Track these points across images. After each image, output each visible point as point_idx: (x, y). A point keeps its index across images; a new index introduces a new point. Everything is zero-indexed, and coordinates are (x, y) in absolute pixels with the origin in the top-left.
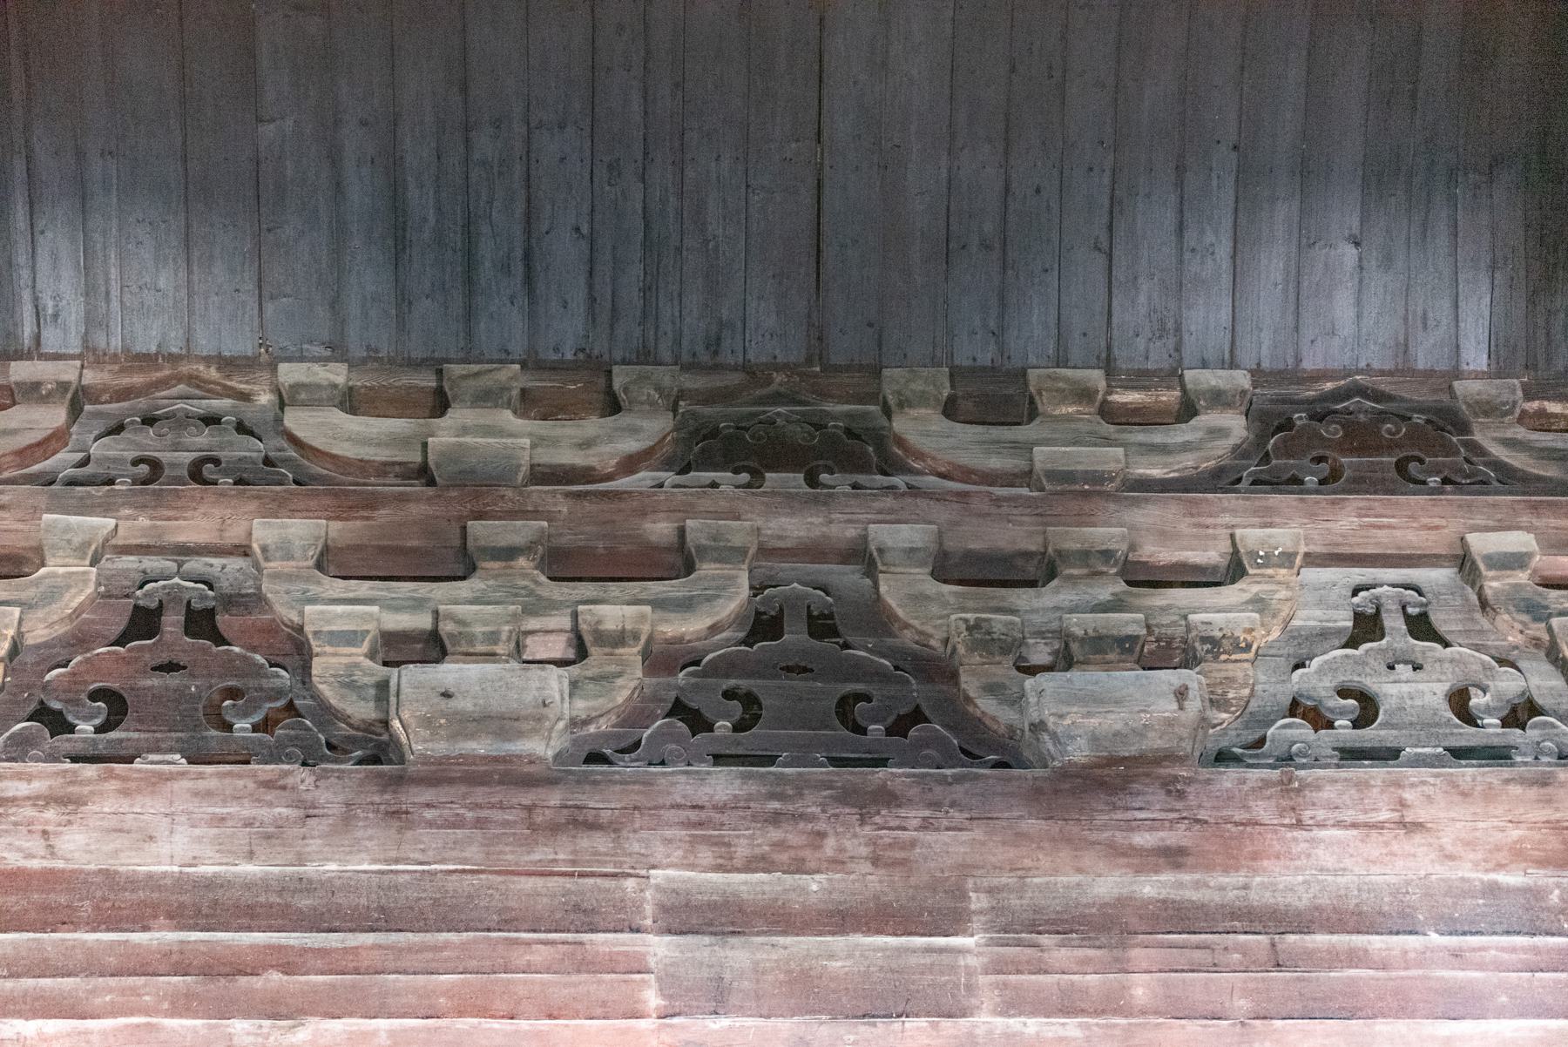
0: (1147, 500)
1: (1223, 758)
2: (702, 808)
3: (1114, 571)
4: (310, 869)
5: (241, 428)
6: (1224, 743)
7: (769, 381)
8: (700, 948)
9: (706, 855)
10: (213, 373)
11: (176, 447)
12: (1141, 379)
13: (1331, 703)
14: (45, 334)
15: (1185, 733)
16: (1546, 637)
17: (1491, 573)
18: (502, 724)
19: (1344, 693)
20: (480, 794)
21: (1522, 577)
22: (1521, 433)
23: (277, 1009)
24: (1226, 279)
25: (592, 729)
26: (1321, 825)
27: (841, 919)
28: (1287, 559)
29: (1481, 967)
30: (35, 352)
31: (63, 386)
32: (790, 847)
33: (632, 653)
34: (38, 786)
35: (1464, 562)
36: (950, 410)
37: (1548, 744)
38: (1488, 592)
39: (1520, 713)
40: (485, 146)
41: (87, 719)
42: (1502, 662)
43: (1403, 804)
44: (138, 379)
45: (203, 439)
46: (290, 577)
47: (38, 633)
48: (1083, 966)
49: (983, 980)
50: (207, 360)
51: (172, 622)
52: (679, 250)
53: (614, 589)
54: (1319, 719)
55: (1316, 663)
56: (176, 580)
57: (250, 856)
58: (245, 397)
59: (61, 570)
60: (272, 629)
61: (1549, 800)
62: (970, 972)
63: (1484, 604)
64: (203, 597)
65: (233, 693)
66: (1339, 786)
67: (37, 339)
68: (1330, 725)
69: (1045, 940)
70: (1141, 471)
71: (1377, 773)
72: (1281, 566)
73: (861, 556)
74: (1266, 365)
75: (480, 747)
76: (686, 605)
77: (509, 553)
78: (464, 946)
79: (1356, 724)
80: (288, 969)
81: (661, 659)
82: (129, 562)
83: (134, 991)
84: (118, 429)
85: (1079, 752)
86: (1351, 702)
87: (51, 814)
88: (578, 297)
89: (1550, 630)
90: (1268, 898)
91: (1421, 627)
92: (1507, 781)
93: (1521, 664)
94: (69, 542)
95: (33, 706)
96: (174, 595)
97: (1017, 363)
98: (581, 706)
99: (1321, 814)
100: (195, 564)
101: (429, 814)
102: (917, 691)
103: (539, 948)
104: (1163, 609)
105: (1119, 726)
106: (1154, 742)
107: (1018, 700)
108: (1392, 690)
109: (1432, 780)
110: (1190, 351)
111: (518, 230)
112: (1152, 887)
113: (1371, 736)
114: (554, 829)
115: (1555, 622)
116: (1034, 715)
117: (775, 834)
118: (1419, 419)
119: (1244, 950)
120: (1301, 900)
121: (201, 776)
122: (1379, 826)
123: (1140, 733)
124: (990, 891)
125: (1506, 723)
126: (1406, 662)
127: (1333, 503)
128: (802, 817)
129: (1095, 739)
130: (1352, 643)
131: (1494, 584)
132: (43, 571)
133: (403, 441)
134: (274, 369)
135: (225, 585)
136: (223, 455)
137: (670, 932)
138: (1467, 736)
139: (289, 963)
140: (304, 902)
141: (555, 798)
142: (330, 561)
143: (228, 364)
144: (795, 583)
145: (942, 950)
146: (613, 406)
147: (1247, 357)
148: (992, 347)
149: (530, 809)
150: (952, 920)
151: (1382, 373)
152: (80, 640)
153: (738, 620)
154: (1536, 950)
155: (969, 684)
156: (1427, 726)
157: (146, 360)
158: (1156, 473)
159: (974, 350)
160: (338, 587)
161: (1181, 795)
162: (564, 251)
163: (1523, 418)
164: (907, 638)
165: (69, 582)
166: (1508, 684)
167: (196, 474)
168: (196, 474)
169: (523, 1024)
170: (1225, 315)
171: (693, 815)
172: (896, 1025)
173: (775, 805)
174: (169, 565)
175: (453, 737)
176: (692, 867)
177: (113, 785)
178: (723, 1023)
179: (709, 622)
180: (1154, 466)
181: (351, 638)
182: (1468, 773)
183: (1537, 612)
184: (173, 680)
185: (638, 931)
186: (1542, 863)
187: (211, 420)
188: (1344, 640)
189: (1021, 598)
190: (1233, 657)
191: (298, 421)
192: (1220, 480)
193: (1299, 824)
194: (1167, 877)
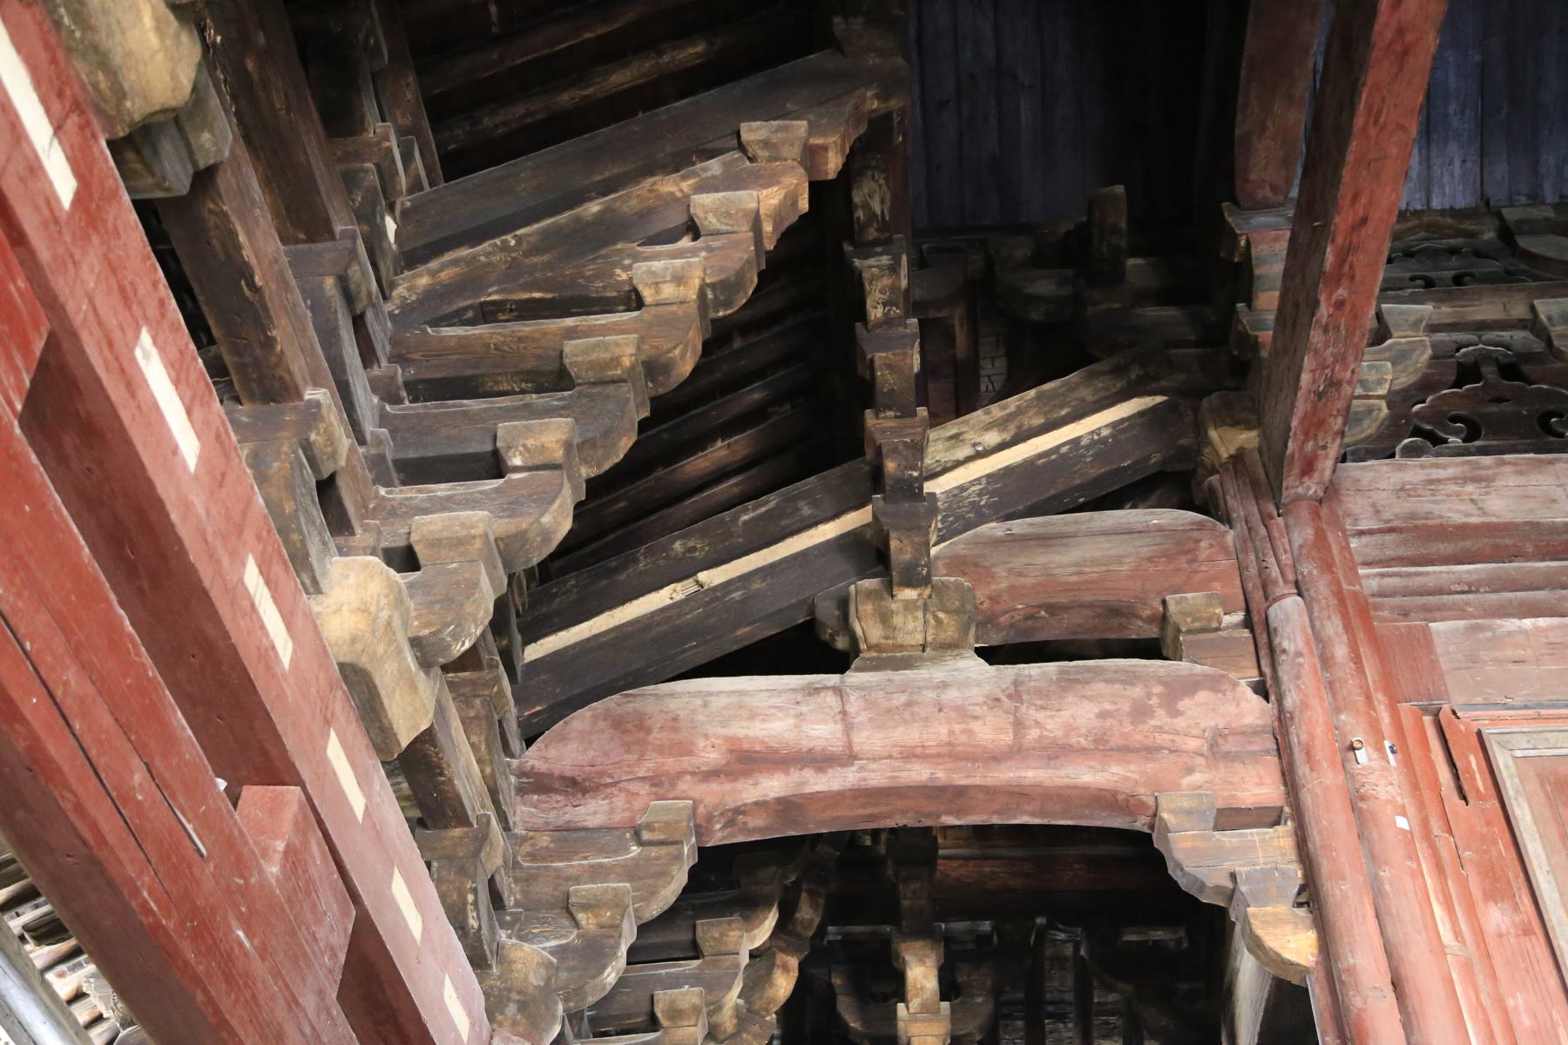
34: (1450, 472)
50: (1442, 212)
51: (1489, 372)
56: (1481, 346)
58: (1470, 235)
59: (1404, 340)
64: (1506, 356)
87: (1470, 488)
94: (1407, 321)
96: (1486, 357)
132: (1389, 342)
136: (1474, 270)
165: (1413, 347)
168: (1458, 280)
174: (1471, 337)
177: (1508, 469)
187: (1454, 251)
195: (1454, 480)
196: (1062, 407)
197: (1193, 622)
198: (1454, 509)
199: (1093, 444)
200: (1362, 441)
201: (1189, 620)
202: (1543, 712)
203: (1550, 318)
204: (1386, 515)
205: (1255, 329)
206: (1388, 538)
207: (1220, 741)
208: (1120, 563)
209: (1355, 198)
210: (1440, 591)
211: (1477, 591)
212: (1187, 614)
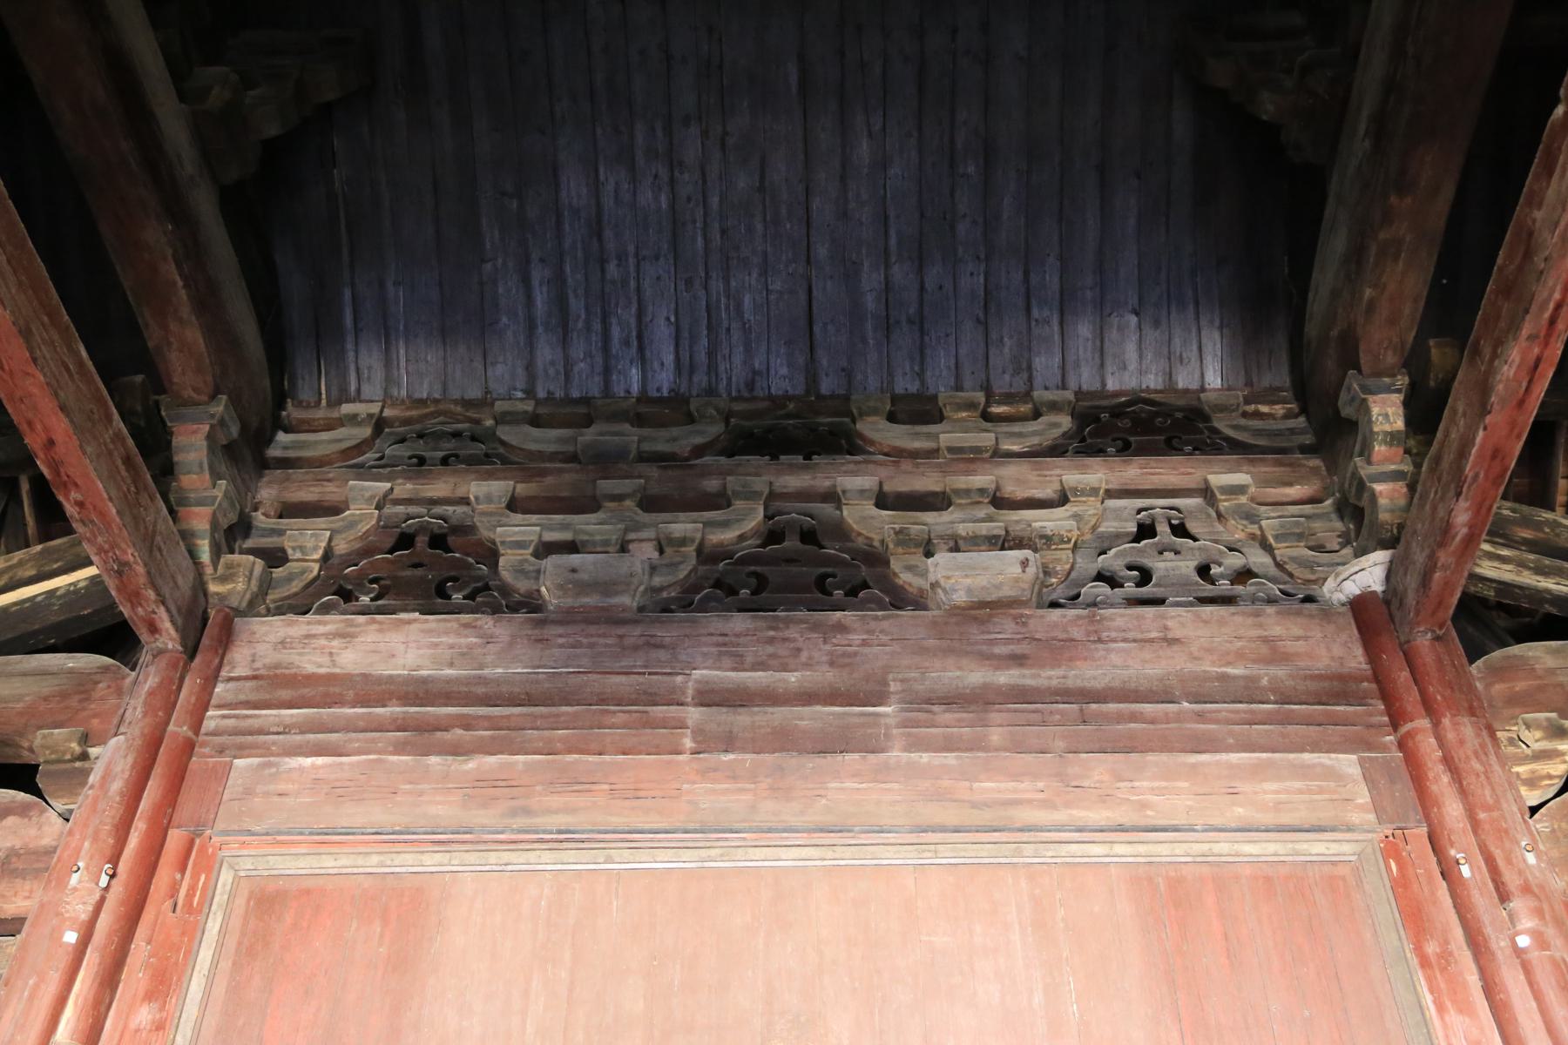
0: (1009, 463)
1: (1054, 605)
2: (726, 635)
3: (986, 501)
4: (486, 672)
5: (474, 439)
6: (1054, 597)
7: (785, 406)
8: (722, 715)
9: (727, 662)
10: (459, 409)
11: (435, 449)
12: (1008, 398)
13: (1122, 574)
14: (363, 388)
15: (1026, 586)
16: (1259, 533)
17: (1223, 497)
18: (606, 587)
19: (1130, 568)
20: (592, 629)
21: (1243, 499)
22: (1243, 422)
23: (456, 750)
24: (1057, 337)
25: (665, 595)
26: (1114, 641)
27: (808, 697)
28: (1094, 491)
29: (1217, 722)
30: (358, 398)
31: (370, 416)
32: (780, 657)
33: (690, 550)
35: (1206, 492)
36: (892, 418)
37: (1261, 594)
38: (1221, 508)
39: (1244, 575)
40: (612, 269)
41: (366, 594)
42: (1231, 550)
43: (1166, 628)
44: (414, 413)
45: (449, 446)
46: (491, 514)
47: (341, 547)
48: (959, 724)
49: (895, 731)
50: (456, 402)
51: (422, 541)
52: (728, 330)
53: (682, 515)
54: (1112, 581)
55: (1113, 551)
56: (426, 518)
57: (451, 665)
58: (477, 422)
59: (358, 512)
60: (480, 543)
61: (1261, 626)
62: (887, 727)
63: (1220, 516)
64: (441, 527)
65: (454, 579)
66: (1126, 619)
67: (359, 391)
68: (1122, 586)
69: (936, 708)
70: (1006, 447)
71: (1149, 611)
72: (1090, 496)
73: (833, 497)
74: (1085, 387)
75: (590, 600)
76: (725, 524)
77: (619, 498)
78: (575, 714)
79: (1139, 585)
80: (467, 727)
81: (708, 556)
82: (400, 509)
83: (373, 741)
84: (402, 441)
85: (960, 598)
86: (1136, 573)
87: (335, 643)
88: (669, 359)
89: (1261, 528)
90: (1079, 683)
91: (1180, 530)
92: (1234, 614)
93: (1243, 550)
94: (363, 496)
95: (334, 588)
96: (423, 528)
97: (932, 391)
98: (657, 581)
99: (1113, 634)
100: (438, 510)
101: (561, 641)
102: (864, 572)
103: (619, 715)
104: (1017, 522)
105: (984, 583)
106: (1007, 592)
107: (924, 574)
108: (1161, 566)
109: (1185, 614)
110: (1038, 381)
111: (633, 321)
112: (1006, 677)
113: (1146, 591)
114: (636, 648)
115: (1264, 523)
116: (932, 578)
117: (770, 649)
118: (1179, 415)
119: (1062, 713)
120: (1098, 684)
121: (427, 621)
122: (1152, 641)
123: (998, 587)
124: (902, 681)
126: (1171, 550)
127: (1125, 461)
128: (785, 640)
129: (969, 591)
130: (1137, 538)
131: (1224, 505)
132: (348, 513)
133: (560, 440)
134: (492, 404)
135: (454, 521)
136: (462, 453)
137: (702, 705)
138: (1208, 590)
139: (467, 724)
140: (481, 690)
141: (637, 631)
142: (514, 505)
143: (468, 404)
144: (794, 514)
145: (870, 714)
146: (690, 419)
147: (1072, 383)
148: (917, 383)
149: (621, 637)
150: (880, 698)
151: (1156, 391)
152: (367, 552)
153: (755, 533)
154: (1252, 712)
155: (895, 565)
156: (1184, 584)
157: (422, 402)
158: (1015, 448)
159: (905, 384)
160: (519, 517)
161: (1024, 624)
162: (662, 332)
163: (1245, 415)
164: (860, 542)
165: (362, 518)
166: (1235, 561)
167: (445, 461)
169: (607, 758)
170: (1057, 360)
171: (721, 639)
172: (839, 757)
173: (772, 633)
174: (422, 510)
175: (578, 595)
176: (719, 669)
177: (375, 626)
178: (731, 756)
179: (738, 533)
180: (1014, 444)
181: (520, 545)
182: (1208, 610)
183: (1252, 518)
184: (419, 572)
185: (682, 704)
186: (1255, 661)
187: (457, 435)
188: (1131, 538)
189: (930, 517)
190: (1060, 547)
191: (505, 433)
192: (1056, 450)
193: (1100, 641)
194: (1015, 672)
195: (327, 636)
196: (57, 561)
197: (50, 754)
198: (311, 662)
199: (68, 593)
200: (288, 597)
201: (47, 752)
202: (279, 838)
203: (477, 498)
204: (258, 665)
205: (178, 505)
206: (249, 684)
207: (14, 860)
208: (18, 701)
209: (30, 424)
210: (261, 732)
211: (289, 733)
212: (48, 748)
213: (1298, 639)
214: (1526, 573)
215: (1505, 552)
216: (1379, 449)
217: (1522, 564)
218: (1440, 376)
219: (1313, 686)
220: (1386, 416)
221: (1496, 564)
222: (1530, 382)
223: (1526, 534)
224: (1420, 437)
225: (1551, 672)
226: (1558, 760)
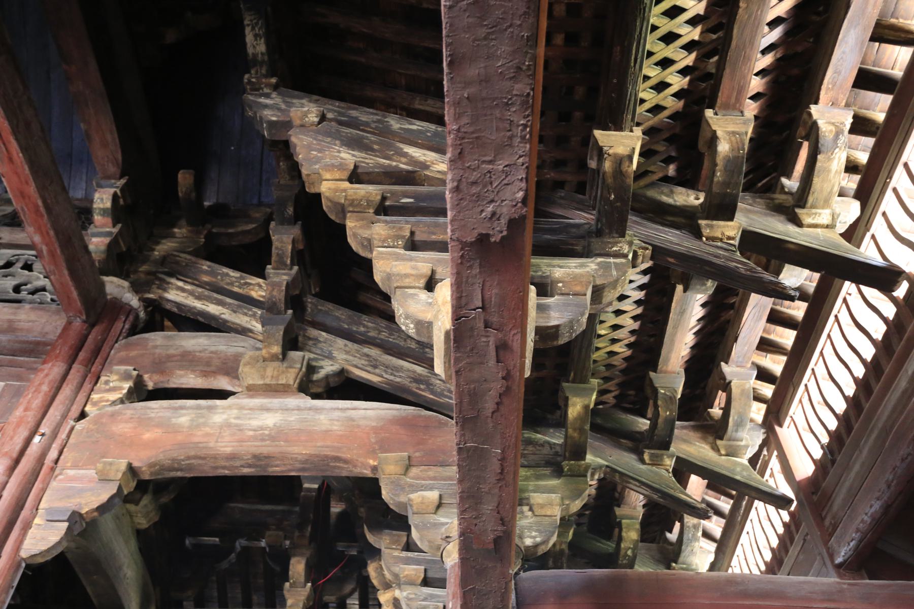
61: (15, 314)
92: (5, 307)
125: (29, 294)
138: (14, 296)
213: (29, 321)
214: (191, 298)
215: (188, 287)
216: (97, 218)
217: (191, 293)
218: (184, 190)
219: (17, 346)
220: (102, 199)
221: (178, 293)
222: (4, 144)
223: (206, 278)
224: (189, 228)
225: (156, 347)
226: (118, 392)
